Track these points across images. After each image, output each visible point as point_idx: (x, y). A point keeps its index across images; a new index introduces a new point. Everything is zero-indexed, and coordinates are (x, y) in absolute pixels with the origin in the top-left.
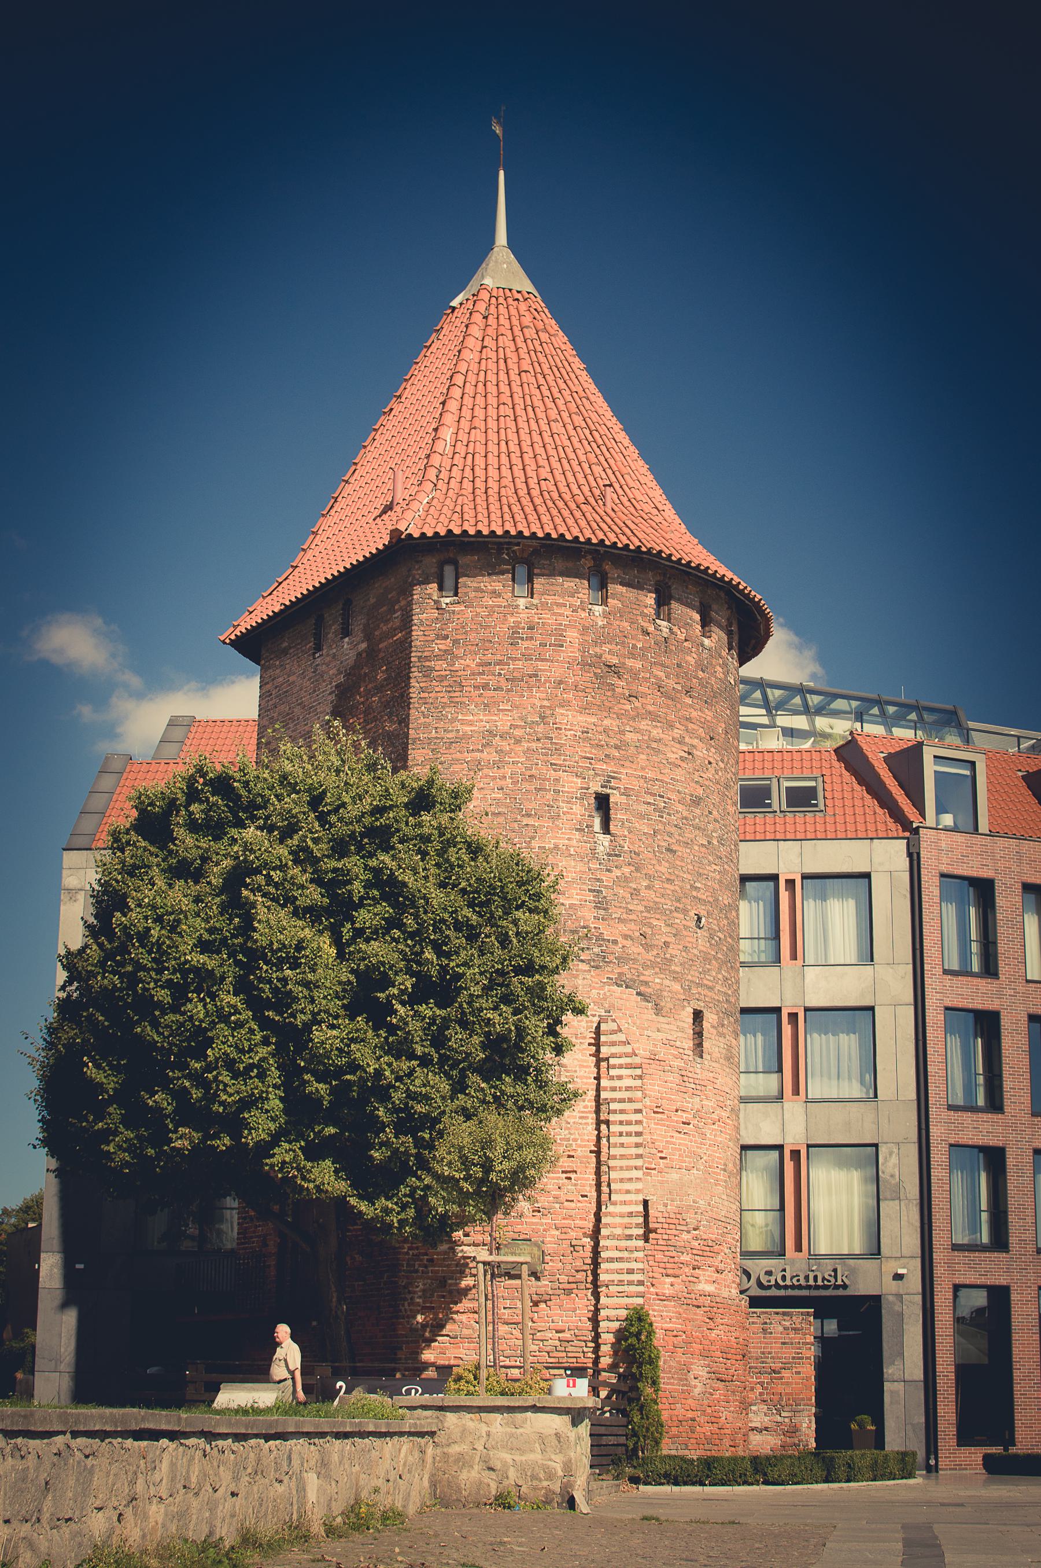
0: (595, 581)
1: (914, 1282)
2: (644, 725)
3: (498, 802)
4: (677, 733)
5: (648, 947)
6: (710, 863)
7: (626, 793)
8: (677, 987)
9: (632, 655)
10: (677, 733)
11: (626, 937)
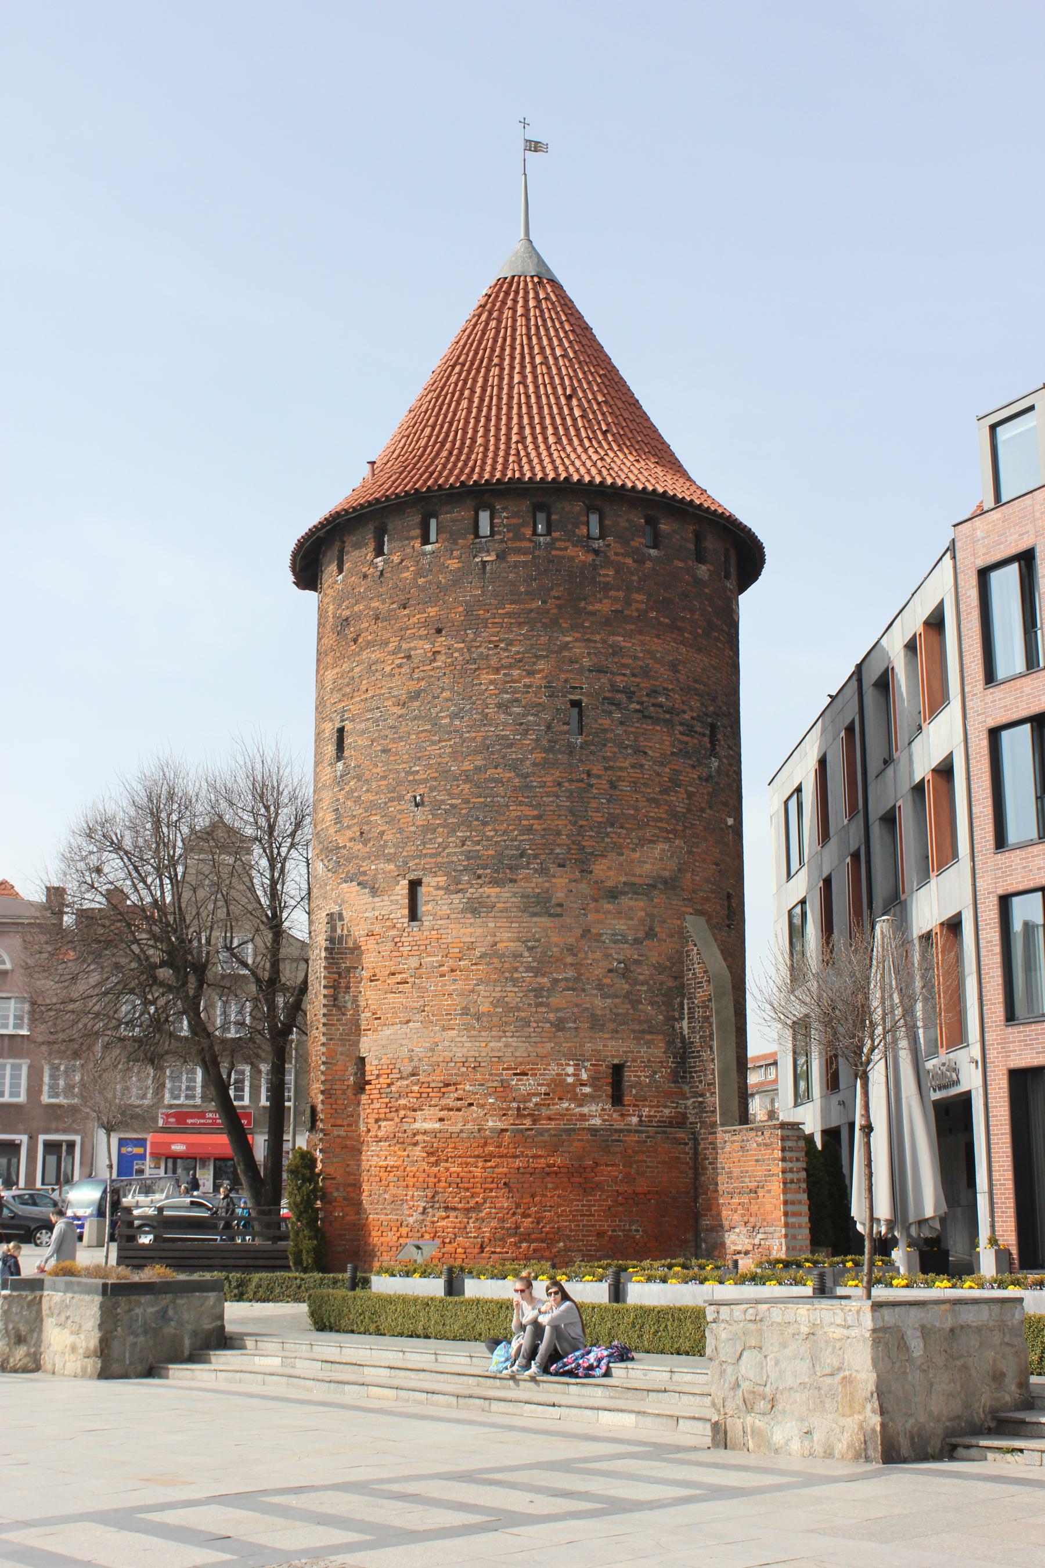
2: (364, 655)
4: (391, 646)
6: (434, 743)
8: (392, 867)
10: (391, 646)
11: (351, 839)
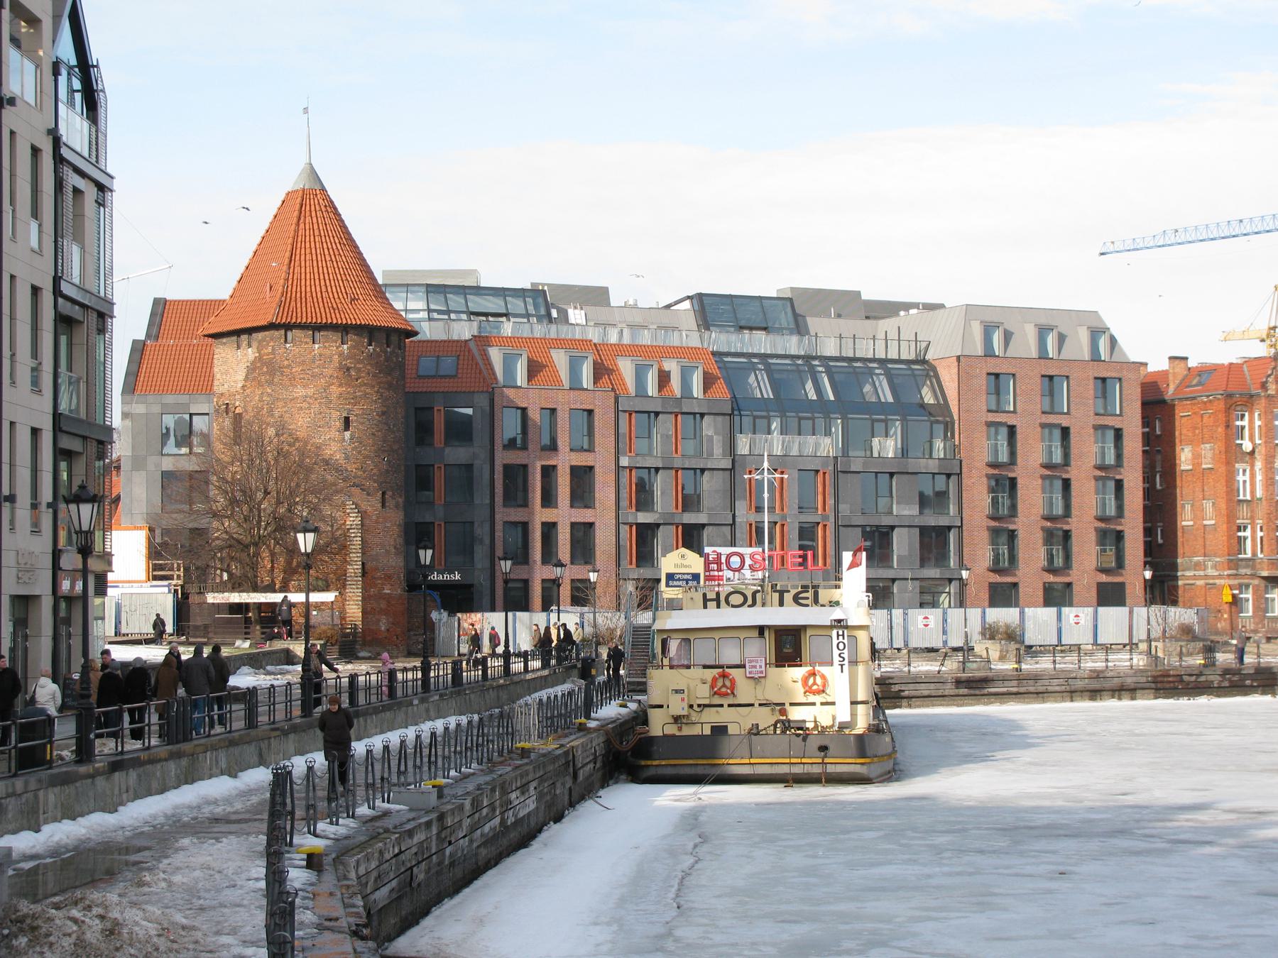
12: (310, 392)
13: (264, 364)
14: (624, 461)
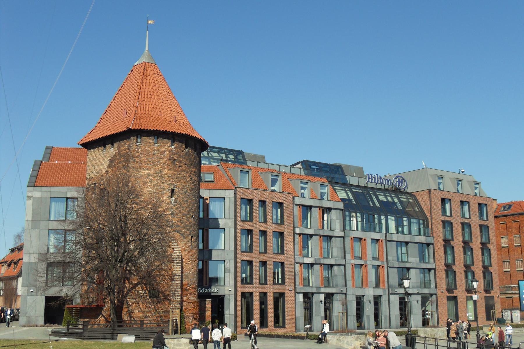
0: (172, 139)
1: (233, 292)
3: (150, 191)
4: (189, 174)
5: (182, 223)
7: (178, 189)
9: (180, 157)
10: (189, 174)
12: (151, 172)
13: (123, 156)
14: (298, 230)
